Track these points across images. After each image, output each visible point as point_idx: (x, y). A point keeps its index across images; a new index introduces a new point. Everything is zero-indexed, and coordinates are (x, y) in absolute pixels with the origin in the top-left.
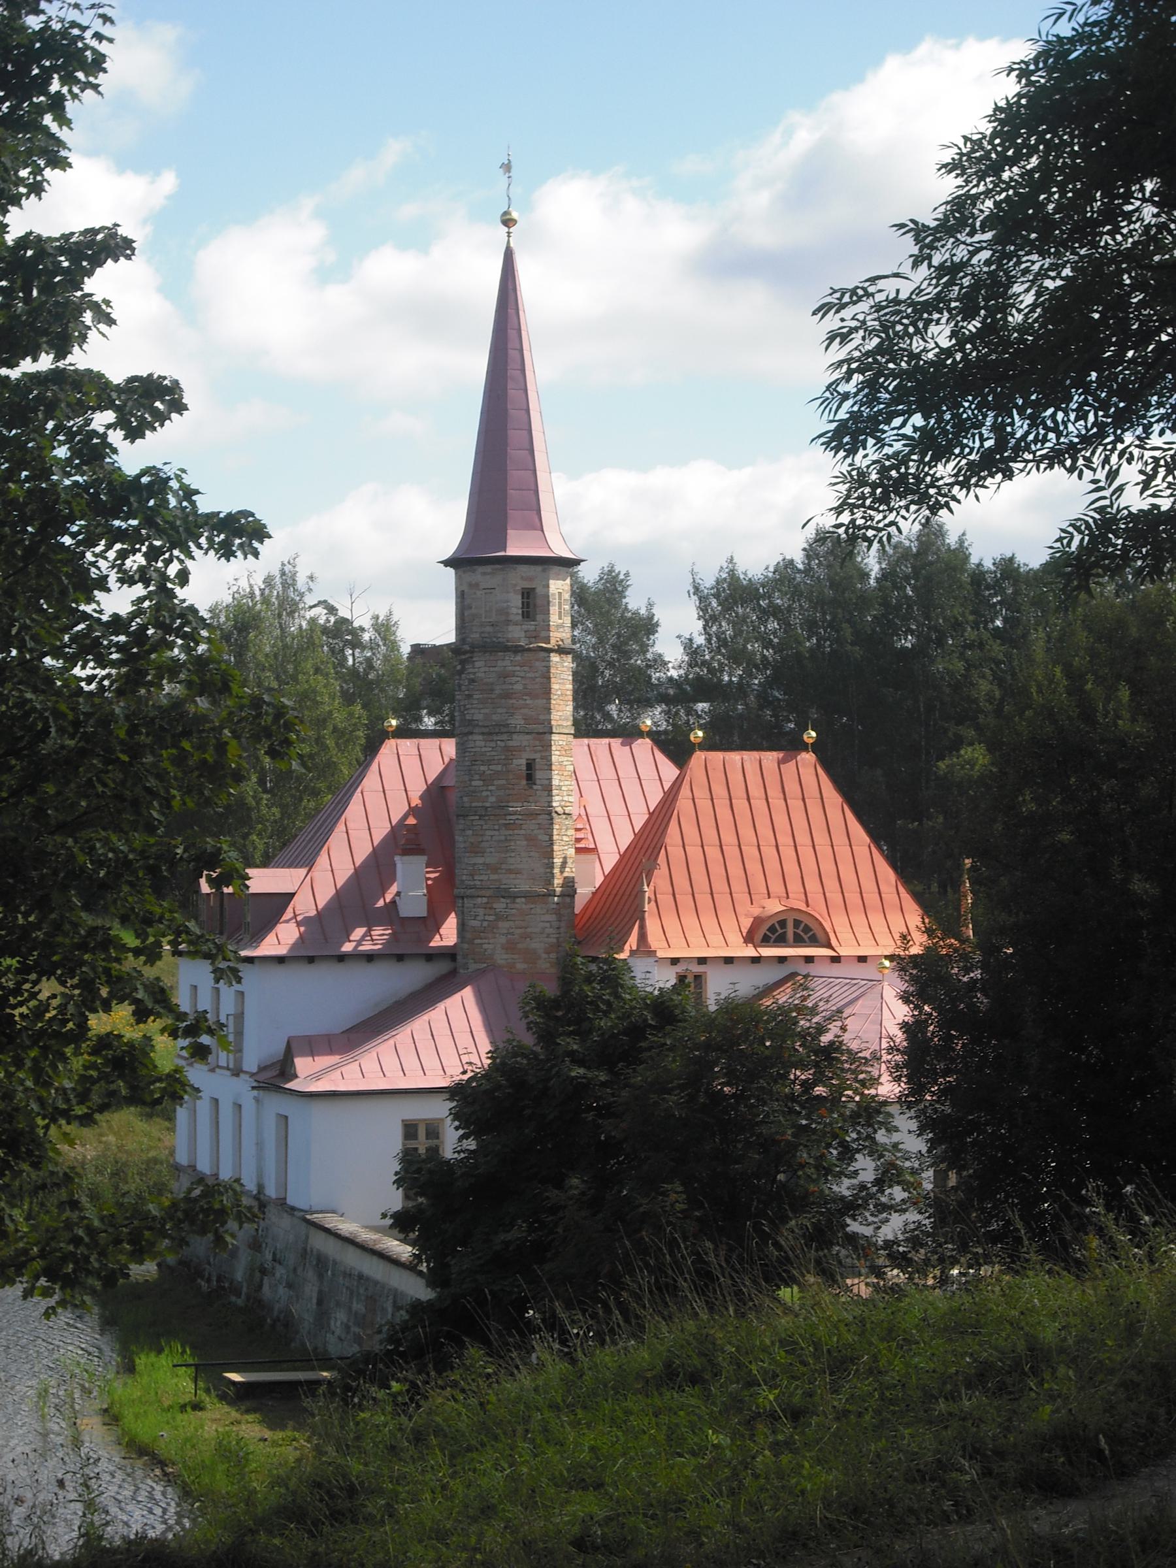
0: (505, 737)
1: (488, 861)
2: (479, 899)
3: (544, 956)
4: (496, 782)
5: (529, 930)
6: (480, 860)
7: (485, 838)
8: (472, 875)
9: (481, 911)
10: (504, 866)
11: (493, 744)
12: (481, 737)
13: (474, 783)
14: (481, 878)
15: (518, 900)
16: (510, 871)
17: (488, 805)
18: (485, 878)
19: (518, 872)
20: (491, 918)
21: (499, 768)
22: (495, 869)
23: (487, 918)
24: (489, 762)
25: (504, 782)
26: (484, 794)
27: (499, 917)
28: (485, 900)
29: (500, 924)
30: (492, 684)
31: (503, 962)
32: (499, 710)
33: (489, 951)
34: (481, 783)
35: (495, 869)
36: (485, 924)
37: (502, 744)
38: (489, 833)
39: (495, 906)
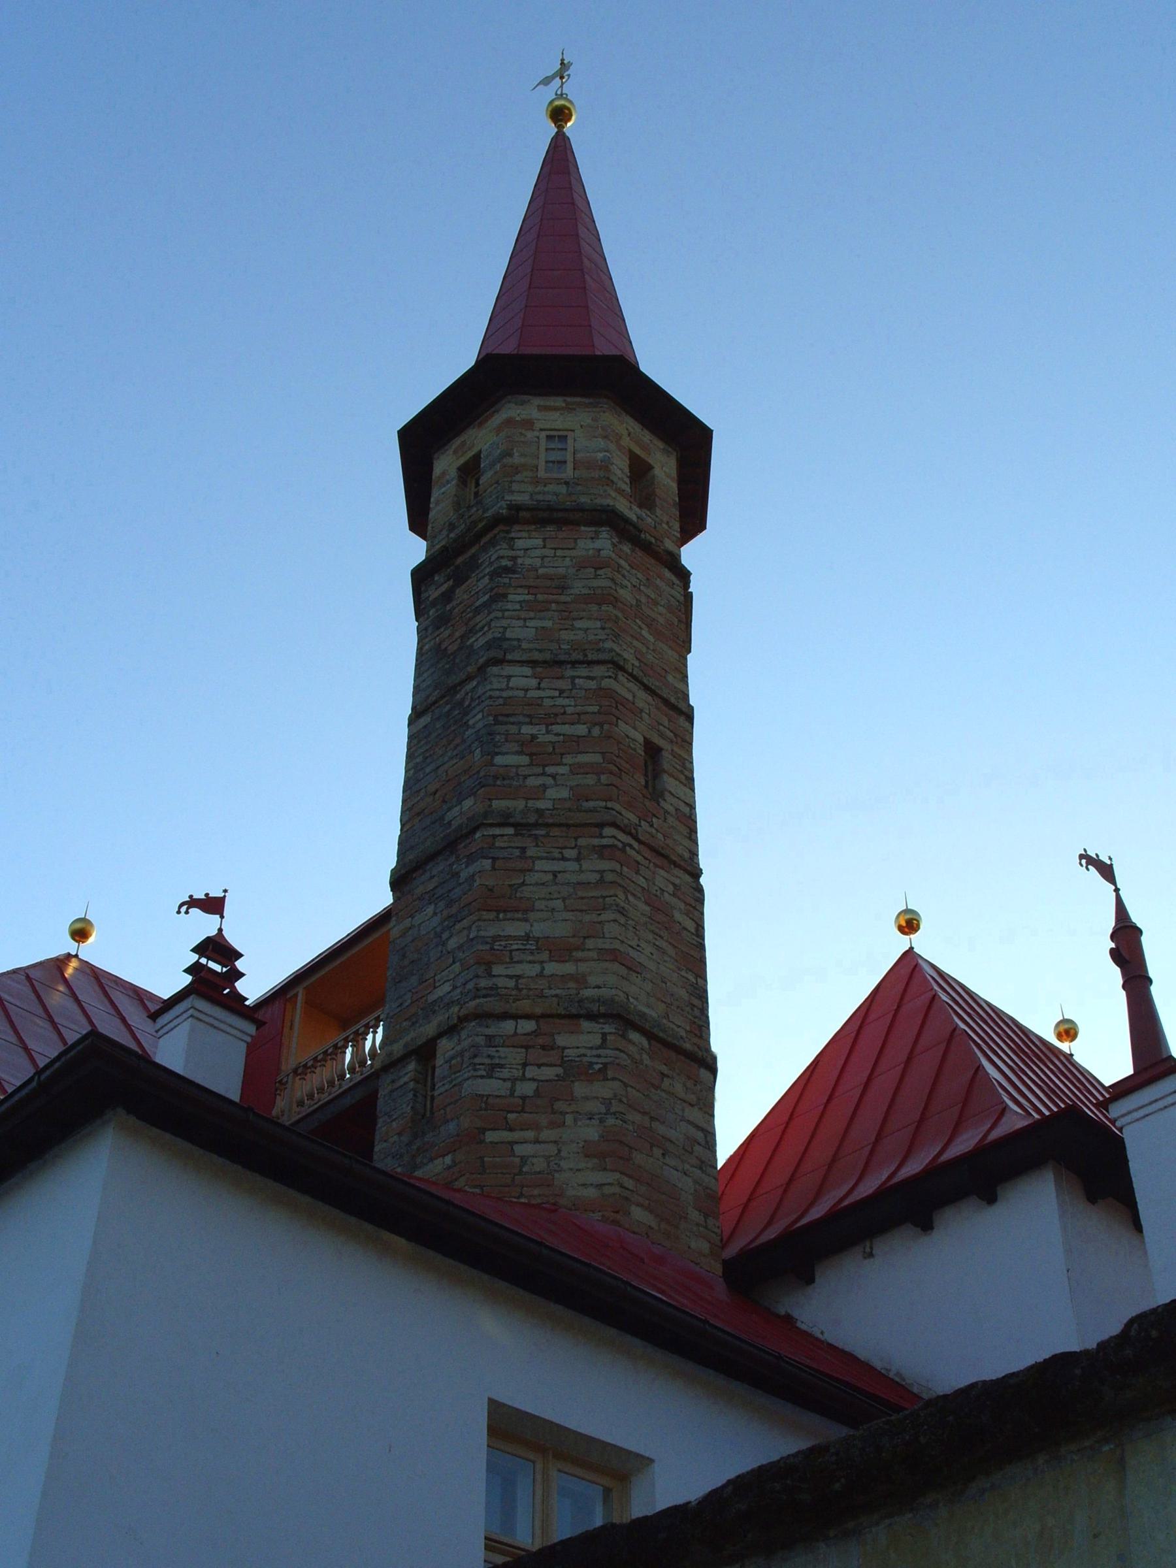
0: (599, 671)
1: (539, 930)
2: (508, 1026)
3: (695, 1215)
4: (568, 759)
5: (661, 1129)
6: (515, 929)
7: (532, 878)
8: (489, 965)
9: (513, 1056)
10: (590, 943)
11: (562, 684)
12: (527, 671)
13: (499, 760)
14: (517, 970)
15: (634, 1036)
16: (614, 956)
17: (541, 805)
18: (531, 970)
19: (633, 968)
20: (549, 1073)
21: (581, 730)
22: (561, 950)
23: (531, 1072)
24: (551, 719)
25: (597, 758)
26: (539, 781)
27: (576, 1070)
28: (528, 1026)
29: (580, 1089)
30: (564, 577)
31: (591, 1193)
32: (578, 624)
33: (539, 1164)
34: (525, 760)
35: (561, 950)
36: (527, 1089)
37: (592, 685)
38: (539, 865)
39: (561, 1040)
